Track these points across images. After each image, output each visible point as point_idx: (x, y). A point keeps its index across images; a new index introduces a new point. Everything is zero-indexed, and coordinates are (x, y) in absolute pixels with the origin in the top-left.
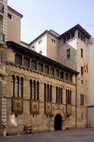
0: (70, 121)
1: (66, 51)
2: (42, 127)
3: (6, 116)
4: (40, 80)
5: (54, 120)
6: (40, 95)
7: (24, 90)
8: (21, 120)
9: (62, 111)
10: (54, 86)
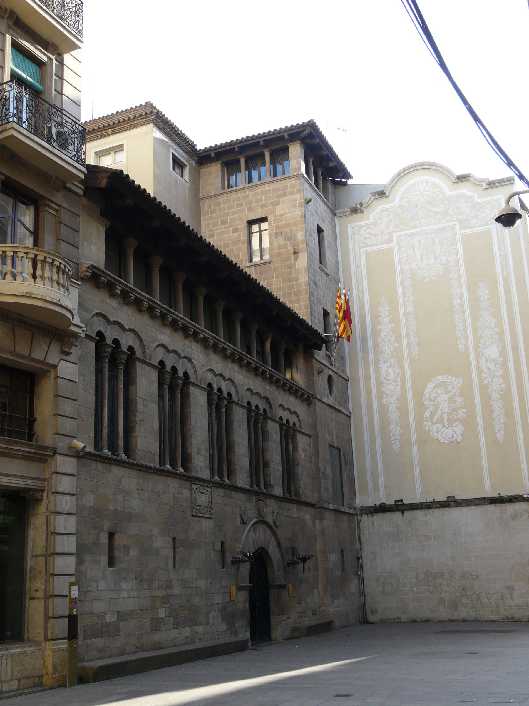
1: (246, 224)
4: (192, 363)
5: (247, 584)
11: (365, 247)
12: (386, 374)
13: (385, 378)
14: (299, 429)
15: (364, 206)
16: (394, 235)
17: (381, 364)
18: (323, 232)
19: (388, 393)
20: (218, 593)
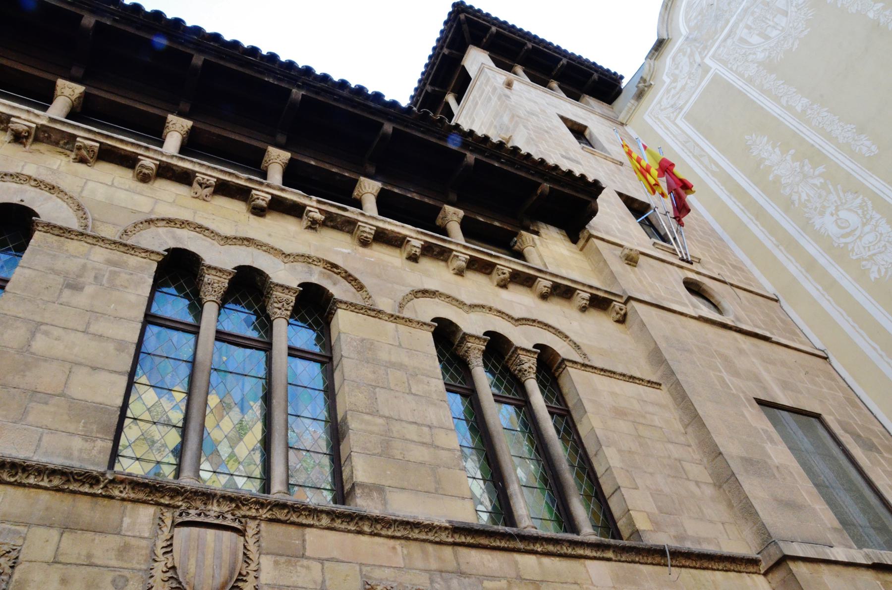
11: (680, 113)
12: (839, 227)
13: (843, 236)
15: (648, 79)
16: (707, 61)
17: (817, 222)
18: (587, 129)
19: (870, 253)
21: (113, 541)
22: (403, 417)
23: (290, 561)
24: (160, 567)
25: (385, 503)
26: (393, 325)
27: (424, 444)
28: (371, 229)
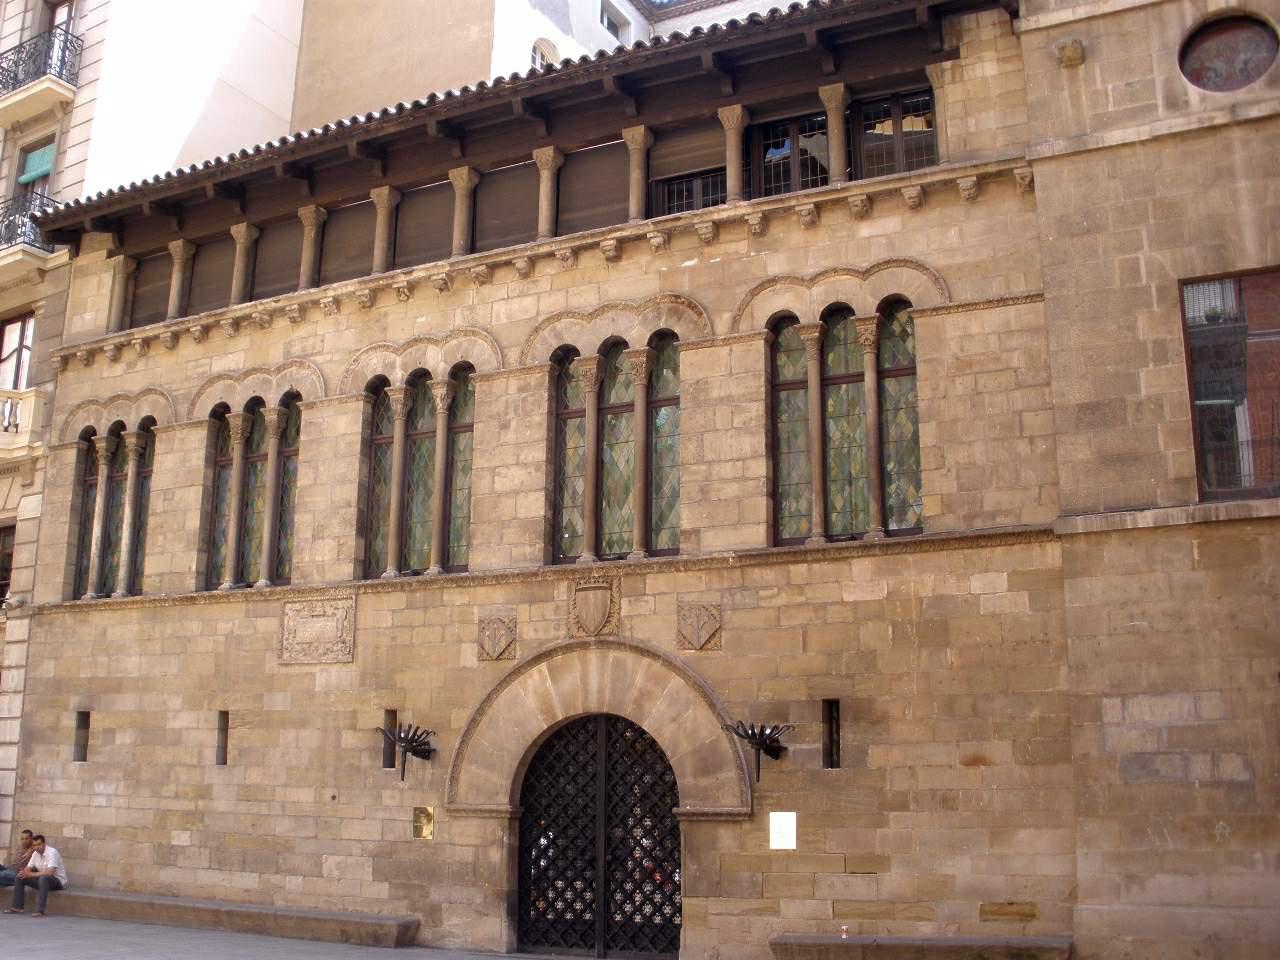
0: (881, 823)
2: (321, 881)
3: (14, 750)
5: (503, 802)
6: (302, 523)
7: (152, 522)
8: (111, 789)
9: (669, 663)
10: (513, 355)
14: (937, 300)
20: (364, 819)
21: (550, 606)
22: (723, 457)
23: (636, 600)
24: (572, 616)
25: (698, 542)
26: (728, 348)
27: (734, 480)
28: (707, 227)
